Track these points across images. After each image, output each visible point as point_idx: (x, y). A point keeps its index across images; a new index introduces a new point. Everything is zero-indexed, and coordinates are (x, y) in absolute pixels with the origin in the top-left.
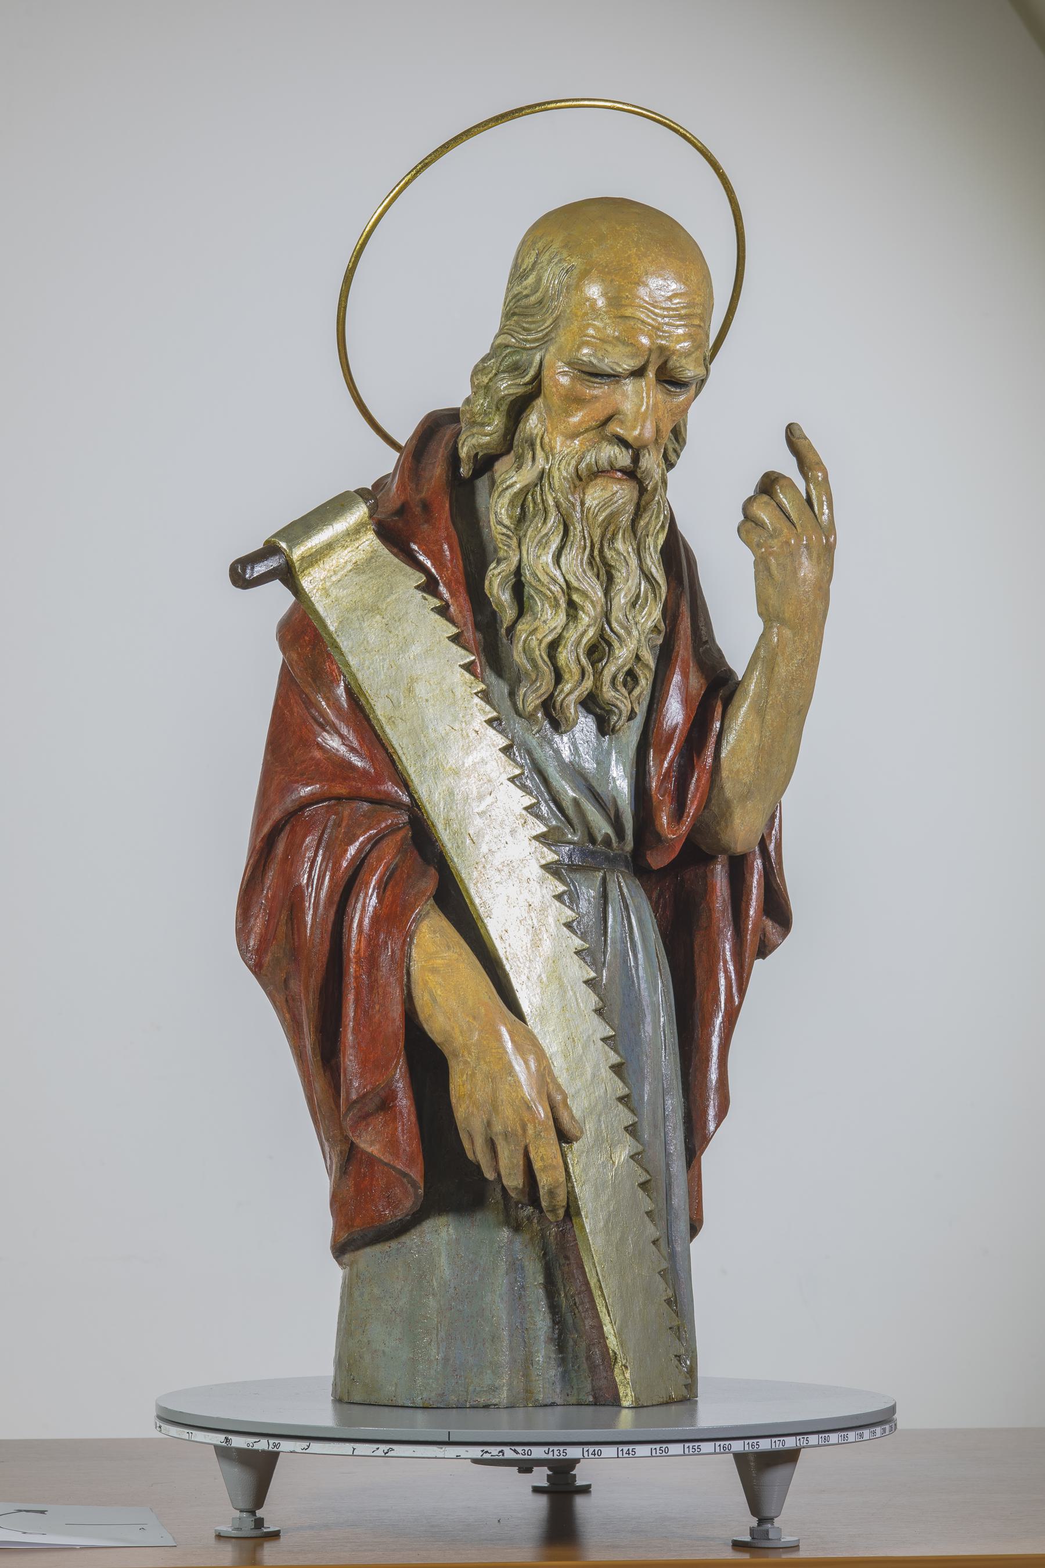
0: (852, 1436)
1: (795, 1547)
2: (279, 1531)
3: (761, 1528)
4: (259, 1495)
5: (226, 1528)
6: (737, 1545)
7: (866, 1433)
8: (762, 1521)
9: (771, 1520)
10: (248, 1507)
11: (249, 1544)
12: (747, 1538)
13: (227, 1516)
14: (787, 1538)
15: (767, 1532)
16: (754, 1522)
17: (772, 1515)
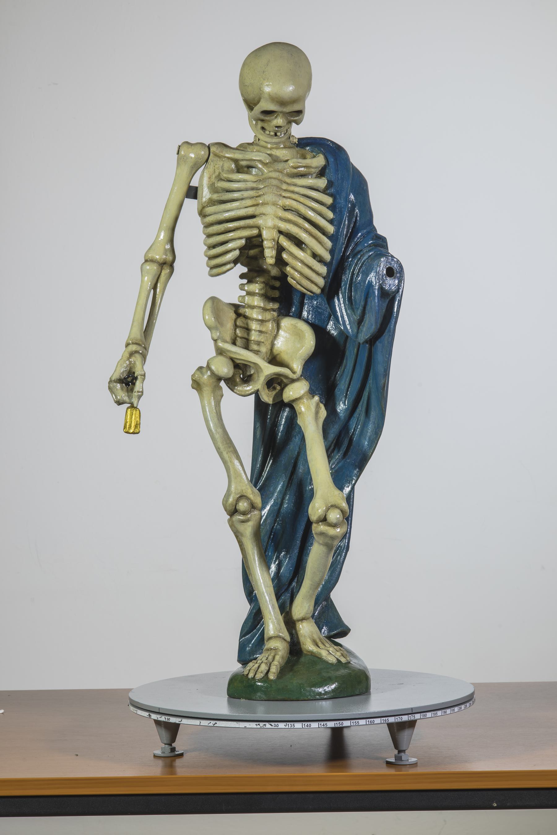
0: (439, 713)
1: (415, 765)
2: (183, 753)
3: (400, 755)
4: (173, 738)
5: (158, 752)
6: (389, 763)
7: (448, 711)
8: (400, 752)
9: (404, 751)
10: (167, 742)
11: (168, 760)
12: (392, 760)
13: (159, 747)
14: (413, 760)
15: (401, 757)
16: (396, 752)
17: (404, 749)
